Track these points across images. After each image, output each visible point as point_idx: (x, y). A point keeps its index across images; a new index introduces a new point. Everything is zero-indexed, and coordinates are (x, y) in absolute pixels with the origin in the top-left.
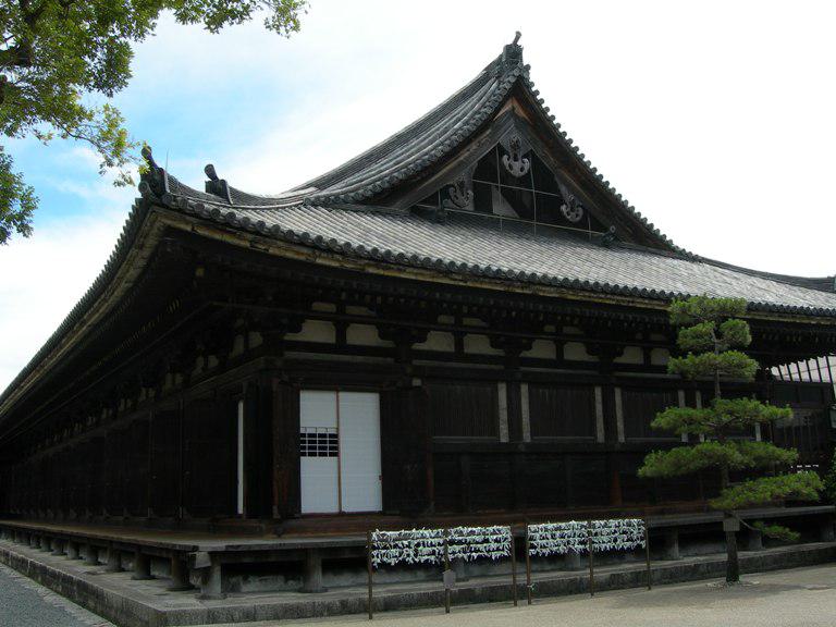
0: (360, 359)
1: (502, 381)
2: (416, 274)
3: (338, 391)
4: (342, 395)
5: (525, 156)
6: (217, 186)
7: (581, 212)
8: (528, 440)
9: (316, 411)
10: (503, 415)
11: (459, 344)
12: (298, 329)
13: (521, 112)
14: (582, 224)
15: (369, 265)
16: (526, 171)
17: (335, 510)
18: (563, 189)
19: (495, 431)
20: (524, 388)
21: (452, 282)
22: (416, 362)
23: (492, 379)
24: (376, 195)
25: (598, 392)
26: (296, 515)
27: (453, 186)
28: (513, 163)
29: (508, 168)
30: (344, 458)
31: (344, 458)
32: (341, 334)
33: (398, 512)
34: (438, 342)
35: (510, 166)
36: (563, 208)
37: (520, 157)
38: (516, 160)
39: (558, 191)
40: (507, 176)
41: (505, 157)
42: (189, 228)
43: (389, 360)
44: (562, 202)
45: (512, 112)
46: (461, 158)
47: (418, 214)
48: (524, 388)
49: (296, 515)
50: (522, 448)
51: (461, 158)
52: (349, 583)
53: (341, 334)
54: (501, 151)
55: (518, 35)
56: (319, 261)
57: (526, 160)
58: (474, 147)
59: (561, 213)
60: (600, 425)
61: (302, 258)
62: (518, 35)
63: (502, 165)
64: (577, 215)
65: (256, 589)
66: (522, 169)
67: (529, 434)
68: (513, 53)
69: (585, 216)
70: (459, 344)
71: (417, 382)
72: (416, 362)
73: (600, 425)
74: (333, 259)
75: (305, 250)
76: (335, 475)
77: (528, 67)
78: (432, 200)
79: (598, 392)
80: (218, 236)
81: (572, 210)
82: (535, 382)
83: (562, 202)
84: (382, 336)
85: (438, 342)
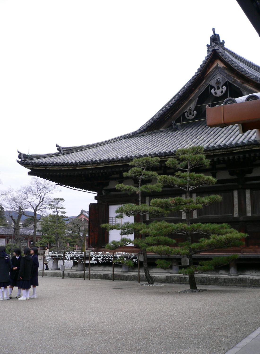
2: (91, 166)
6: (59, 148)
13: (221, 65)
25: (236, 194)
26: (103, 247)
27: (187, 112)
28: (217, 91)
29: (214, 94)
35: (216, 93)
38: (218, 88)
41: (213, 89)
45: (217, 67)
46: (191, 98)
47: (172, 128)
51: (191, 98)
52: (101, 270)
54: (212, 87)
55: (213, 30)
56: (63, 169)
57: (224, 87)
58: (197, 91)
60: (236, 208)
62: (213, 30)
66: (222, 92)
67: (196, 215)
68: (215, 39)
73: (236, 208)
77: (223, 42)
79: (236, 194)
80: (38, 168)
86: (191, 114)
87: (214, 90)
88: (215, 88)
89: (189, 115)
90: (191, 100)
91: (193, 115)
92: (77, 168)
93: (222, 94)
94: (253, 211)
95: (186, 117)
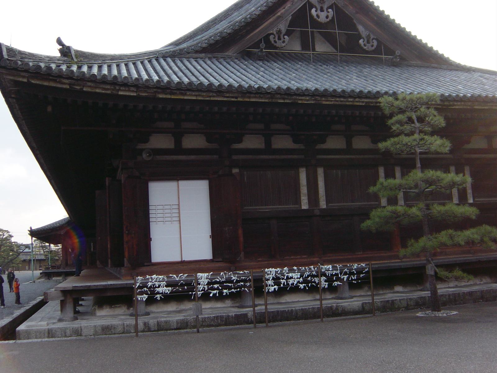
0: (193, 157)
1: (302, 166)
2: (196, 96)
3: (178, 180)
4: (182, 183)
5: (331, 7)
6: (66, 51)
7: (375, 43)
8: (324, 207)
9: (161, 193)
10: (304, 190)
11: (268, 143)
12: (147, 141)
14: (377, 51)
15: (159, 93)
16: (330, 18)
17: (179, 260)
18: (361, 28)
19: (298, 201)
20: (320, 172)
21: (225, 99)
22: (235, 157)
23: (295, 166)
24: (211, 45)
26: (146, 264)
27: (272, 34)
29: (315, 17)
30: (181, 223)
31: (181, 223)
32: (178, 142)
33: (221, 260)
34: (252, 142)
35: (318, 16)
36: (361, 41)
37: (325, 8)
38: (322, 10)
39: (357, 30)
40: (316, 24)
41: (313, 10)
42: (25, 80)
43: (215, 157)
44: (360, 37)
46: (279, 14)
47: (247, 55)
48: (320, 172)
49: (146, 264)
50: (317, 212)
51: (279, 14)
53: (178, 142)
54: (312, 6)
56: (121, 93)
57: (330, 10)
58: (289, 5)
59: (359, 45)
61: (109, 92)
63: (311, 16)
64: (372, 46)
65: (109, 314)
66: (327, 17)
67: (325, 203)
69: (379, 46)
70: (268, 143)
71: (235, 171)
72: (235, 157)
74: (129, 91)
75: (108, 87)
76: (179, 236)
78: (256, 45)
80: (46, 84)
81: (368, 42)
82: (328, 166)
83: (360, 37)
84: (208, 141)
85: (252, 142)
86: (279, 39)
87: (316, 11)
88: (316, 7)
89: (277, 40)
90: (279, 17)
91: (284, 42)
92: (161, 96)
93: (328, 20)
94: (328, 202)
95: (273, 42)
